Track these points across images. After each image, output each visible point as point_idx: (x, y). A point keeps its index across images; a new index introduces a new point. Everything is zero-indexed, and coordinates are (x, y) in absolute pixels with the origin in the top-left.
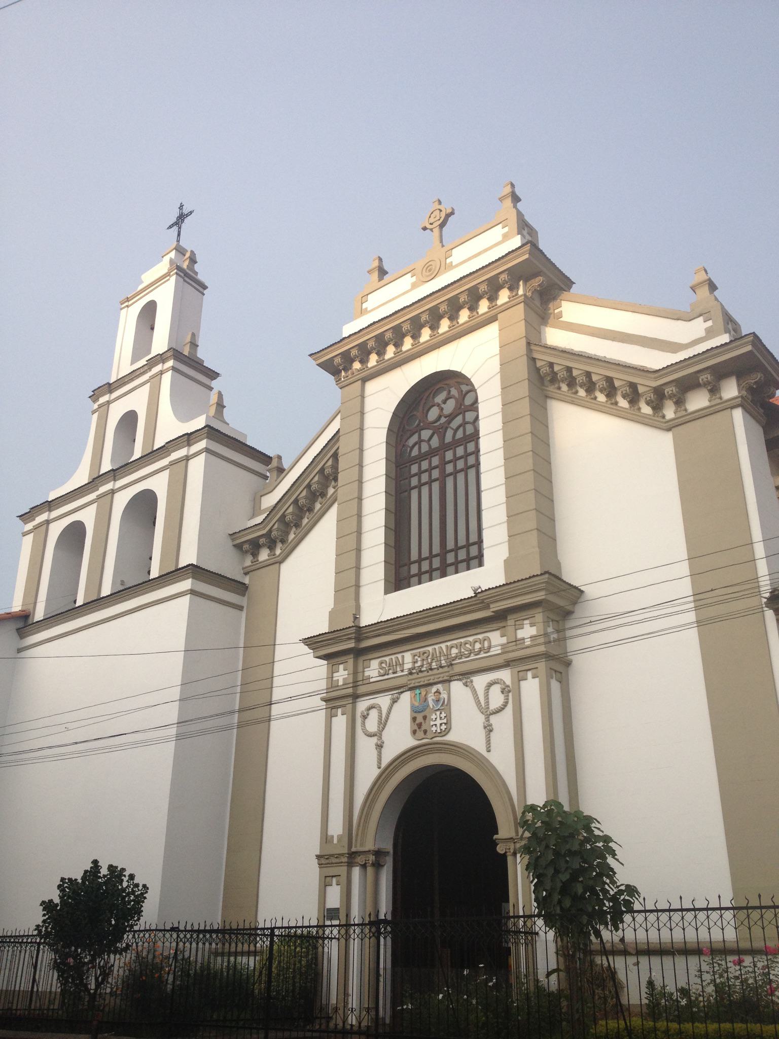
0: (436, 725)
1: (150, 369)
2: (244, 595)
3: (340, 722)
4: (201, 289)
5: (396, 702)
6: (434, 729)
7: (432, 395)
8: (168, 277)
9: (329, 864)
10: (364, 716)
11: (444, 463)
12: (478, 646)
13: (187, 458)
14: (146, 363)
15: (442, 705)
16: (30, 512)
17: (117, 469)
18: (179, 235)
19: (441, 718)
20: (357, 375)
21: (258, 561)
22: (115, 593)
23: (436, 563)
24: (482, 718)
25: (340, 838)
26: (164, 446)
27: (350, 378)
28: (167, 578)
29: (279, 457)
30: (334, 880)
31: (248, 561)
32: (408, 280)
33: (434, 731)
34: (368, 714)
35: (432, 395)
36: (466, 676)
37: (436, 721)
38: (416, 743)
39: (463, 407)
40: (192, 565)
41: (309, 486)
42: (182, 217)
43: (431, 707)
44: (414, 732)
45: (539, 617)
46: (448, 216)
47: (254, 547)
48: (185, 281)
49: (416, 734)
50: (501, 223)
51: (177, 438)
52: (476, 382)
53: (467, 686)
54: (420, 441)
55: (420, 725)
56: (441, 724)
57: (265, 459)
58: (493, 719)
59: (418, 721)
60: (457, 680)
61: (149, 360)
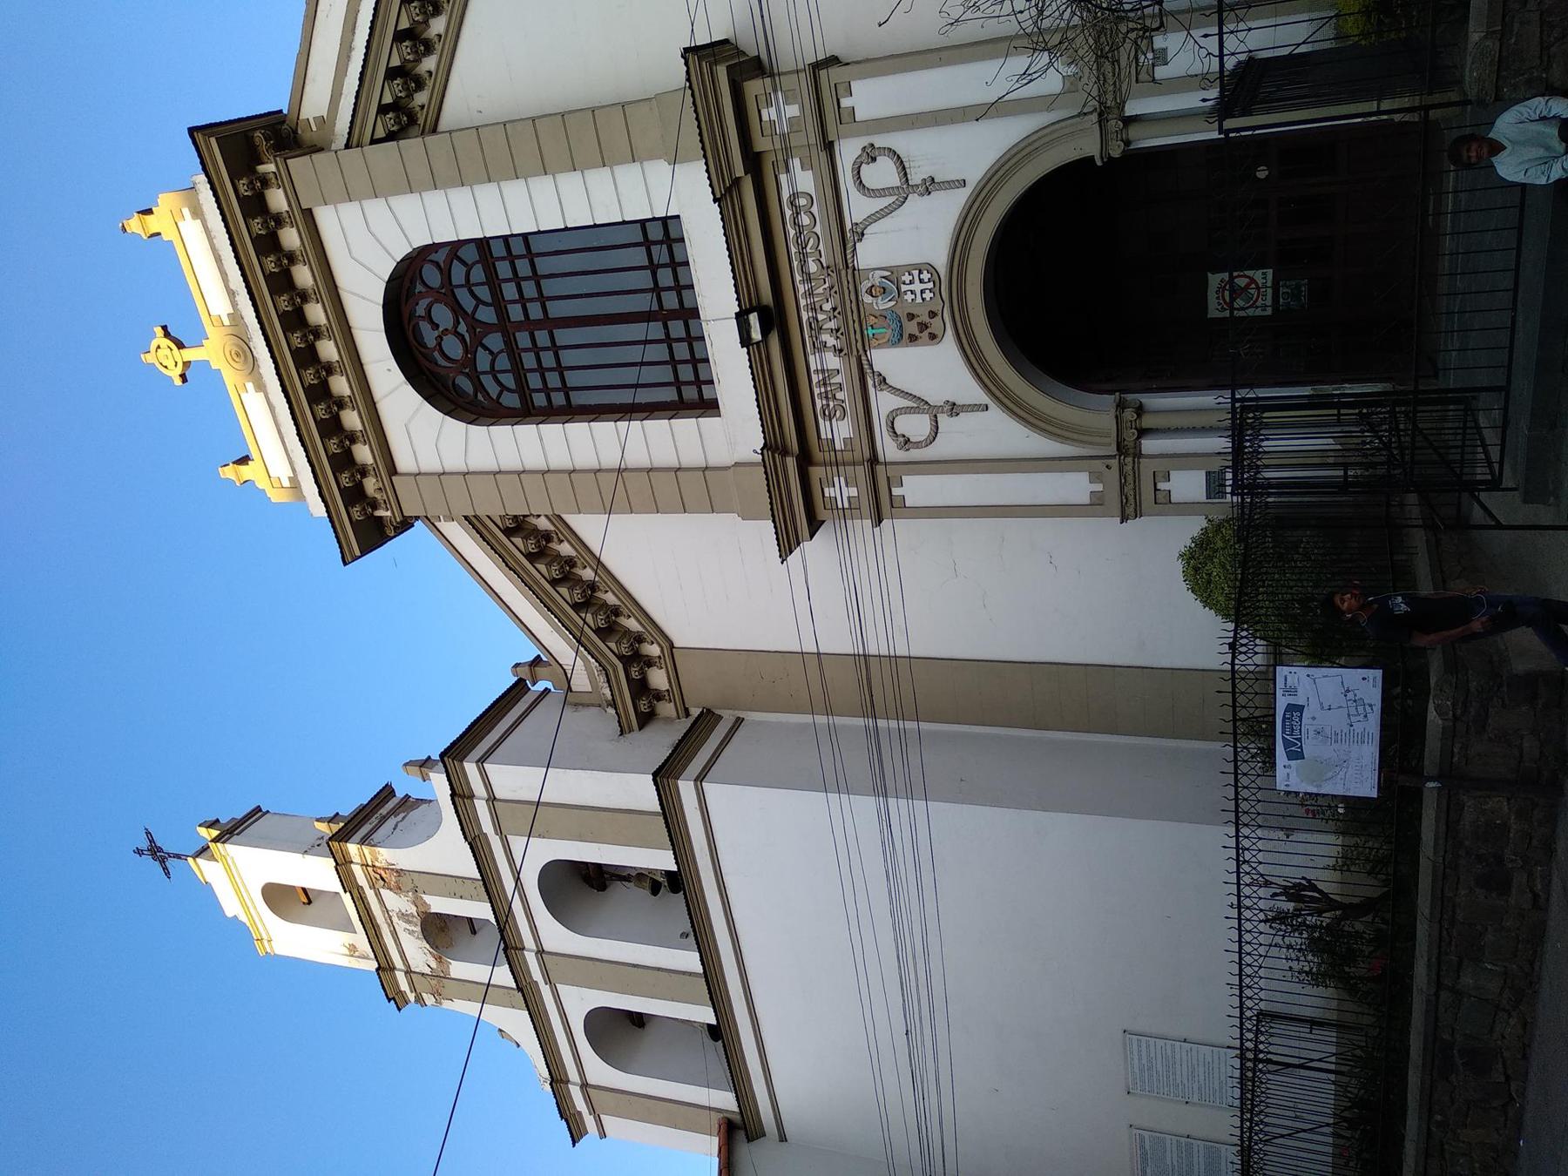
0: (922, 292)
1: (359, 889)
2: (720, 717)
3: (915, 489)
4: (260, 814)
5: (884, 379)
6: (928, 295)
7: (423, 350)
9: (1135, 496)
10: (906, 443)
11: (529, 325)
12: (805, 220)
13: (492, 799)
14: (348, 894)
15: (891, 282)
16: (567, 1121)
18: (178, 856)
19: (911, 282)
20: (383, 481)
21: (668, 691)
22: (699, 948)
23: (677, 329)
24: (913, 199)
25: (1095, 477)
26: (470, 844)
27: (388, 497)
28: (678, 839)
29: (517, 665)
30: (1161, 486)
31: (666, 709)
33: (932, 295)
34: (904, 436)
35: (423, 350)
36: (846, 237)
37: (917, 291)
38: (950, 332)
39: (443, 291)
40: (655, 775)
41: (554, 583)
42: (155, 851)
43: (893, 303)
44: (933, 337)
45: (754, 88)
46: (167, 334)
47: (641, 688)
48: (237, 834)
49: (936, 333)
51: (458, 816)
52: (402, 251)
53: (863, 234)
54: (493, 372)
55: (923, 326)
56: (921, 281)
57: (518, 689)
58: (916, 178)
59: (916, 331)
61: (344, 888)
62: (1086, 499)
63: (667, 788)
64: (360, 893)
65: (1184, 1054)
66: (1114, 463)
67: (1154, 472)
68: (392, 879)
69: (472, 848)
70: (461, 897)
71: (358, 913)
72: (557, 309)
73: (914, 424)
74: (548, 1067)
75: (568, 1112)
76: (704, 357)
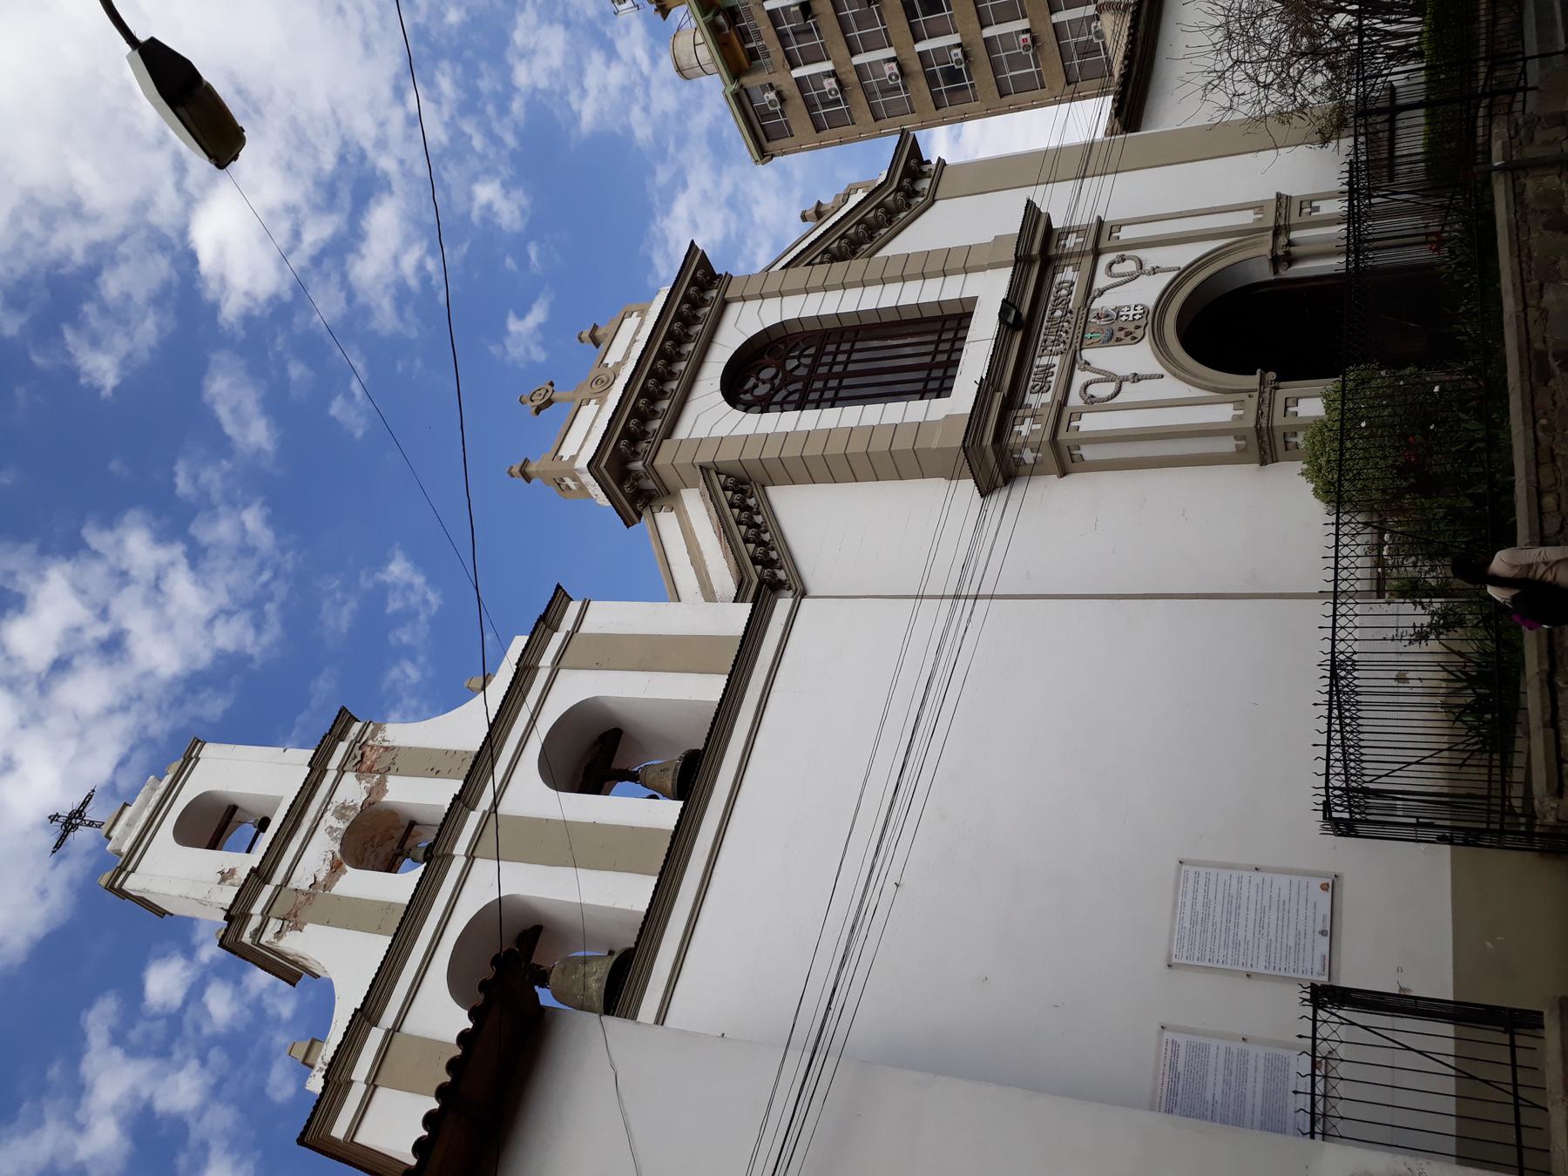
0: (1134, 315)
1: (324, 772)
8: (194, 760)
12: (1064, 292)
17: (461, 791)
25: (1239, 404)
26: (518, 669)
32: (588, 412)
36: (1089, 294)
41: (739, 523)
44: (1134, 338)
46: (552, 384)
50: (623, 319)
53: (1102, 294)
55: (1127, 334)
58: (1147, 267)
60: (1093, 301)
62: (1230, 419)
63: (767, 598)
64: (318, 777)
65: (1253, 890)
66: (1256, 394)
67: (1286, 399)
68: (371, 756)
69: (516, 674)
70: (437, 773)
71: (296, 797)
72: (851, 367)
73: (1102, 390)
74: (371, 986)
75: (338, 1073)
76: (949, 386)
